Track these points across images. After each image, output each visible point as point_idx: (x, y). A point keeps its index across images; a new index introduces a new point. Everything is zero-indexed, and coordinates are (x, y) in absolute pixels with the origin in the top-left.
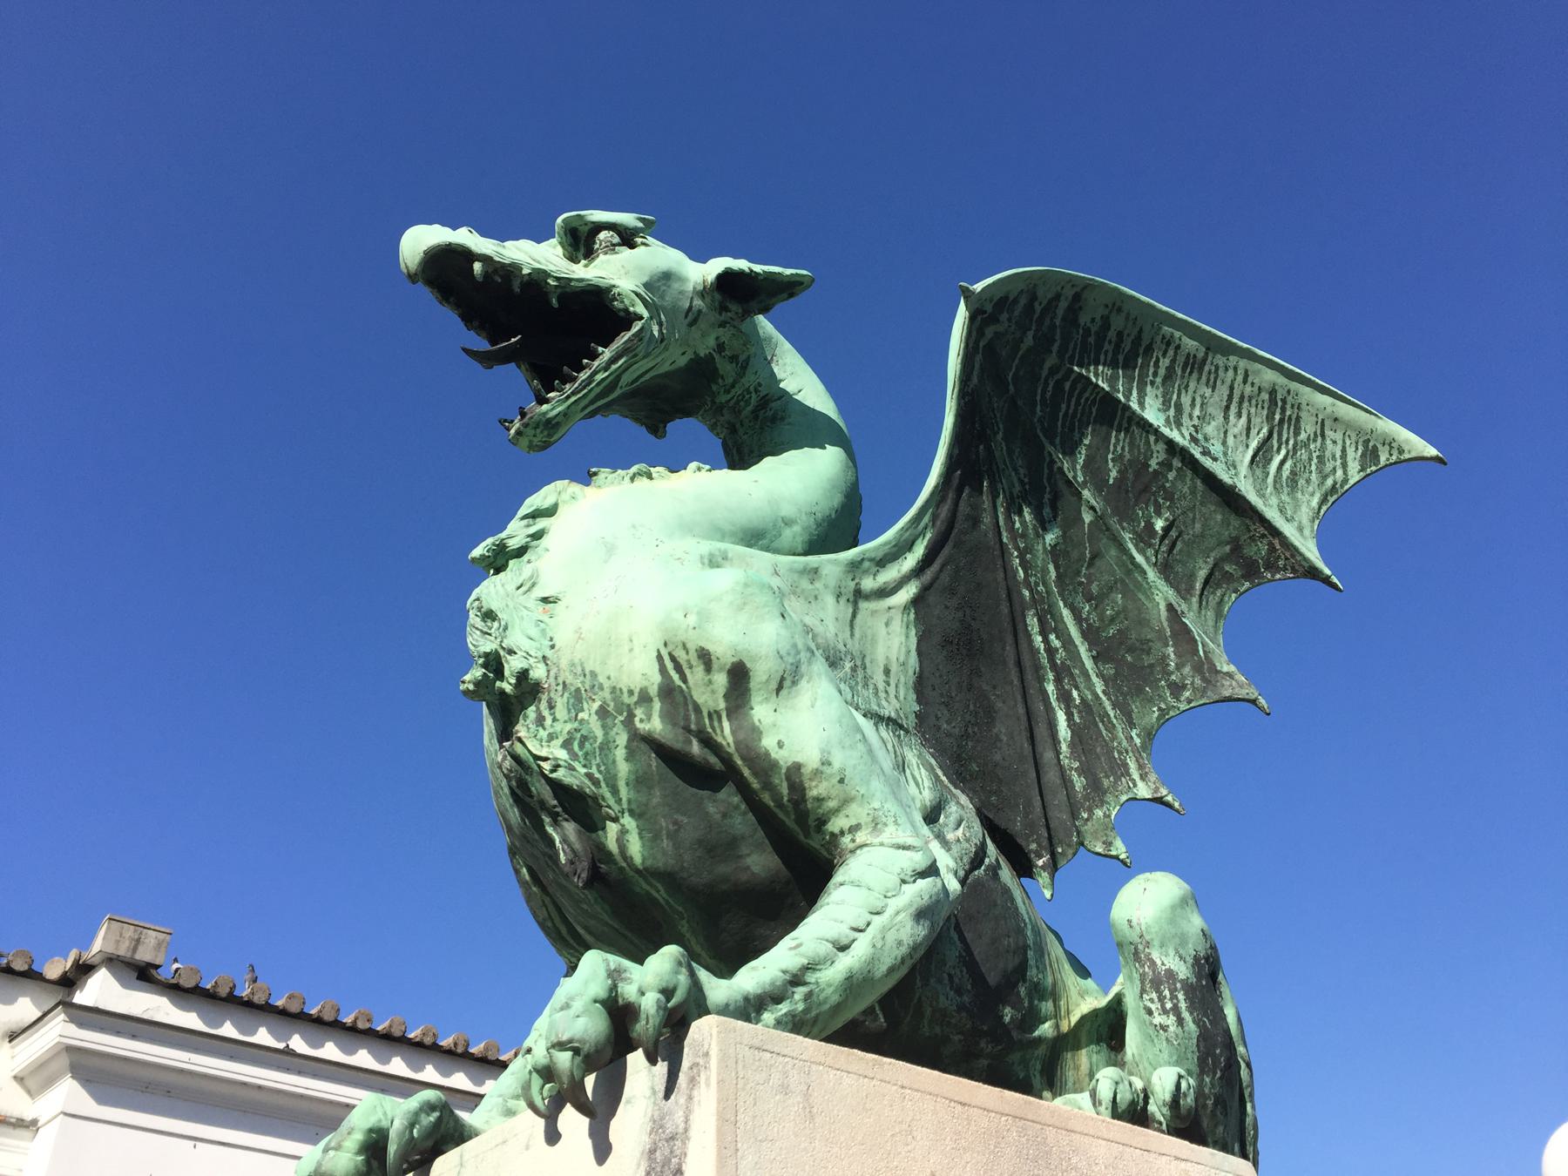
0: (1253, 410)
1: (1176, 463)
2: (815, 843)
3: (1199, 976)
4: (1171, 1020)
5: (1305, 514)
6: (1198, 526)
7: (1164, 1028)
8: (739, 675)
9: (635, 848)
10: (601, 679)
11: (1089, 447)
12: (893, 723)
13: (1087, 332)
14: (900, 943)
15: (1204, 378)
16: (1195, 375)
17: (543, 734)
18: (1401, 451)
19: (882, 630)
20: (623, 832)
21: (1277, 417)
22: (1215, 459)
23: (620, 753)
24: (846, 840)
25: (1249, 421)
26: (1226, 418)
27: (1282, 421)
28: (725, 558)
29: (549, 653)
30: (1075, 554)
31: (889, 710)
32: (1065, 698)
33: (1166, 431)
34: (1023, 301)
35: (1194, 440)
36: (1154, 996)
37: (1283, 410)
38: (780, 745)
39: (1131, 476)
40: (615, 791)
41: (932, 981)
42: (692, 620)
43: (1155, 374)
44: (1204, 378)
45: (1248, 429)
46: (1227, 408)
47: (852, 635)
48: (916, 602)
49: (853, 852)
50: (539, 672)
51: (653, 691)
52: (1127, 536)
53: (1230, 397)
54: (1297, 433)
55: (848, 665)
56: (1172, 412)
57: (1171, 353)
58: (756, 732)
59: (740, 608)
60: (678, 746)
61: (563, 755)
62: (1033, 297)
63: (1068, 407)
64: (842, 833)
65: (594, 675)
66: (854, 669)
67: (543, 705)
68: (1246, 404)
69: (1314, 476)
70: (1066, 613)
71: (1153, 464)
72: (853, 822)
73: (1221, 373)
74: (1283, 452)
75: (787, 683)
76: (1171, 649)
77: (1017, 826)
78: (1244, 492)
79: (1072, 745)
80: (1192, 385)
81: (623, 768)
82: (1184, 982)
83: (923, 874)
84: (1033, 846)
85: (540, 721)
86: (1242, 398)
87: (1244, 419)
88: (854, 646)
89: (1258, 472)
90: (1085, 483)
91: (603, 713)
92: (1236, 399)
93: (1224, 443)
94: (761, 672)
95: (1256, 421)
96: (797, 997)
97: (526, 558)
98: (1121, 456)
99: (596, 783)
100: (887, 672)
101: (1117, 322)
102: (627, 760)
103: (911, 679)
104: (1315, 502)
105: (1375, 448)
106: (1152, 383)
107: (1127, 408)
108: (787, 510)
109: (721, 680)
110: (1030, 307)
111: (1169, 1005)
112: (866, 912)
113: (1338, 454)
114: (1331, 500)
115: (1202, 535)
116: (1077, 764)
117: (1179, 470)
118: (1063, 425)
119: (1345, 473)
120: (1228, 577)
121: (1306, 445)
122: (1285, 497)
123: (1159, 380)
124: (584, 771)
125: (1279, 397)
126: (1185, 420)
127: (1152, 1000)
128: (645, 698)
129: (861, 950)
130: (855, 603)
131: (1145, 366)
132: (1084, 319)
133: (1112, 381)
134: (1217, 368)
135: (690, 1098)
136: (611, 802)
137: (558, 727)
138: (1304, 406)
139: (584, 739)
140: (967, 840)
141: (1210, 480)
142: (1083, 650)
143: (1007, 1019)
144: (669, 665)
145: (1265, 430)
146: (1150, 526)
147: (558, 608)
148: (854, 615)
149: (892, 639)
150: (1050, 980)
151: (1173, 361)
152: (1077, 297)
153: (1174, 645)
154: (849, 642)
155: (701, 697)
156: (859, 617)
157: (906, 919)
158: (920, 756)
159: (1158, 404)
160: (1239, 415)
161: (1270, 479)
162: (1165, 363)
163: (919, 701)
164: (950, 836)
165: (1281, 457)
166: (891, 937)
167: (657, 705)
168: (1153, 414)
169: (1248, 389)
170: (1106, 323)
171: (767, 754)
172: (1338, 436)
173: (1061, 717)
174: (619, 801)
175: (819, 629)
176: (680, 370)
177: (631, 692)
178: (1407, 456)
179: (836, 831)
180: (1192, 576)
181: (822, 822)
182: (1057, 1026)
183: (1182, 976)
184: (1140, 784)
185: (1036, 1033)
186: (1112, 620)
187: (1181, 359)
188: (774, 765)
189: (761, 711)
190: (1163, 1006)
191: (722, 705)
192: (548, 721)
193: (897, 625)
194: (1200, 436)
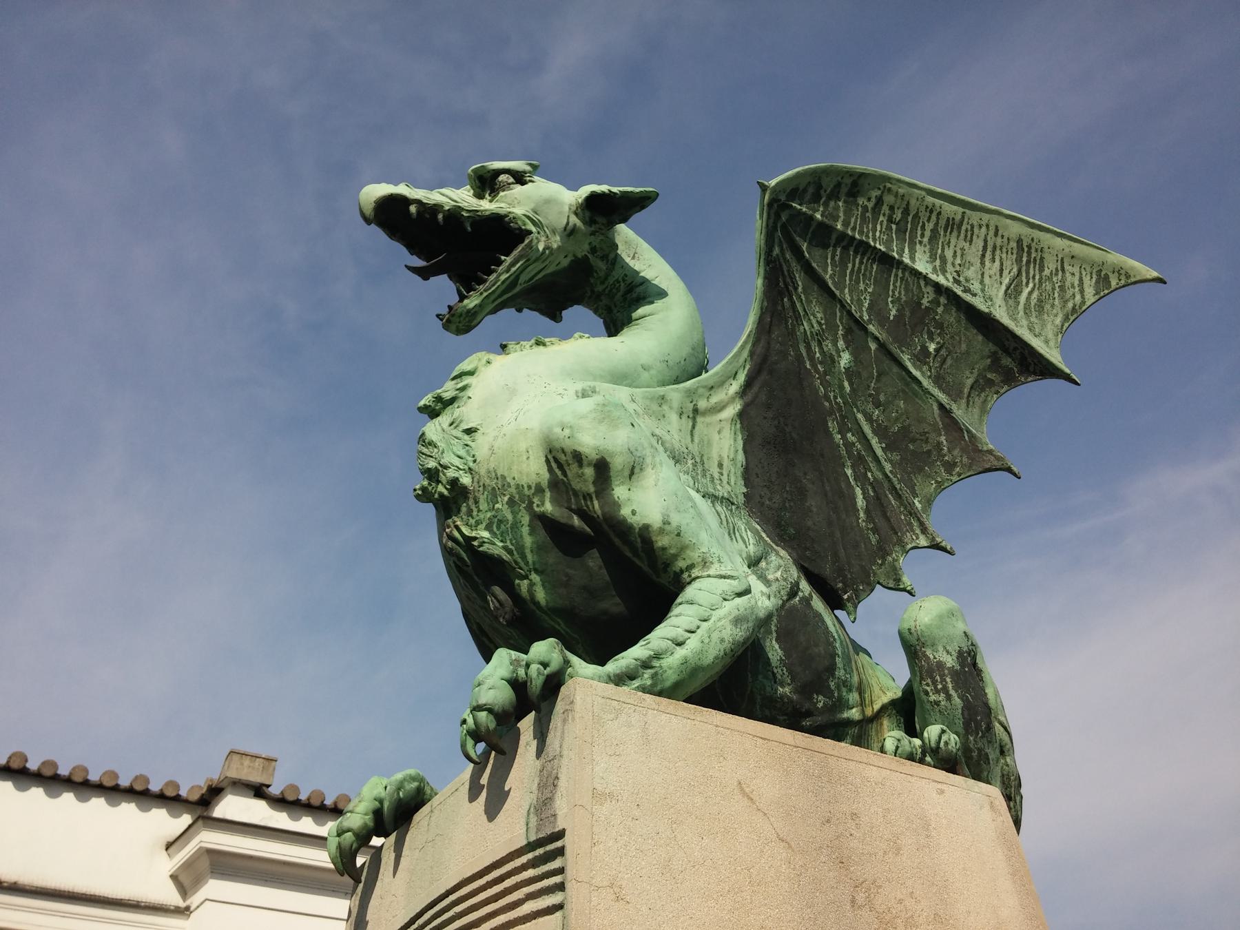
0: (1004, 256)
1: (943, 300)
2: (664, 580)
3: (962, 664)
4: (942, 697)
5: (1050, 331)
6: (964, 346)
7: (937, 703)
9: (541, 595)
10: (508, 480)
11: (871, 294)
13: (865, 208)
14: (722, 640)
15: (962, 235)
16: (955, 233)
17: (472, 521)
18: (1128, 276)
19: (716, 437)
20: (532, 584)
21: (1025, 259)
22: (975, 295)
23: (525, 530)
24: (685, 575)
25: (1002, 264)
26: (983, 263)
27: (1028, 262)
28: (594, 392)
29: (471, 464)
30: (865, 374)
31: (722, 491)
32: (861, 478)
33: (933, 277)
34: (811, 190)
36: (929, 681)
37: (1029, 253)
38: (634, 512)
40: (523, 557)
41: (760, 677)
42: (567, 432)
43: (923, 235)
44: (962, 235)
45: (1001, 270)
46: (983, 256)
47: (692, 440)
48: (741, 415)
49: (689, 583)
50: (466, 480)
51: (545, 484)
52: (906, 359)
53: (985, 248)
54: (1041, 270)
55: (690, 462)
56: (938, 263)
57: (934, 217)
58: (617, 505)
59: (601, 422)
60: (563, 521)
61: (486, 534)
62: (819, 187)
63: (854, 265)
64: (682, 571)
65: (504, 477)
66: (695, 465)
67: (471, 502)
68: (998, 252)
69: (1057, 302)
70: (859, 416)
71: (925, 302)
72: (689, 562)
73: (976, 230)
74: (1031, 285)
75: (637, 470)
76: (943, 439)
77: (827, 570)
78: (998, 317)
79: (867, 511)
80: (953, 242)
81: (528, 541)
82: (951, 669)
83: (740, 595)
84: (840, 585)
86: (995, 248)
87: (997, 263)
88: (694, 449)
89: (1011, 302)
90: (870, 321)
91: (511, 503)
92: (989, 249)
93: (982, 282)
94: (618, 463)
95: (1007, 264)
96: (646, 676)
97: (456, 405)
98: (899, 299)
99: (510, 552)
100: (720, 465)
101: (889, 199)
102: (530, 534)
103: (740, 471)
104: (1058, 321)
105: (1107, 277)
106: (921, 242)
108: (645, 359)
109: (589, 472)
111: (940, 687)
112: (700, 624)
113: (1076, 283)
114: (1072, 318)
115: (967, 353)
116: (871, 526)
117: (945, 305)
118: (851, 280)
119: (1083, 297)
120: (990, 383)
121: (1049, 278)
122: (1033, 319)
123: (926, 240)
124: (501, 544)
125: (1025, 244)
126: (949, 267)
127: (928, 685)
128: (539, 490)
129: (693, 643)
130: (694, 419)
131: (914, 230)
133: (888, 243)
134: (972, 226)
135: (563, 732)
136: (522, 564)
137: (482, 516)
138: (1046, 249)
139: (500, 522)
140: (785, 580)
142: (874, 441)
143: (820, 705)
144: (554, 465)
145: (1015, 270)
146: (925, 349)
147: (477, 435)
148: (693, 427)
149: (724, 443)
150: (856, 679)
151: (937, 224)
152: (855, 184)
153: (946, 434)
154: (690, 446)
155: (576, 485)
156: (697, 428)
157: (726, 623)
159: (926, 257)
162: (929, 227)
163: (746, 485)
164: (770, 577)
165: (1029, 289)
166: (715, 636)
167: (548, 494)
168: (922, 265)
169: (999, 240)
170: (880, 201)
171: (625, 520)
172: (1076, 270)
173: (858, 491)
174: (527, 563)
175: (667, 437)
176: (565, 270)
177: (529, 487)
178: (1133, 280)
179: (678, 570)
180: (962, 385)
181: (667, 565)
182: (863, 711)
183: (949, 665)
184: (922, 537)
185: (845, 715)
186: (897, 419)
187: (942, 223)
188: (630, 527)
189: (620, 492)
190: (936, 687)
191: (592, 489)
192: (475, 513)
193: (727, 433)
194: (961, 279)
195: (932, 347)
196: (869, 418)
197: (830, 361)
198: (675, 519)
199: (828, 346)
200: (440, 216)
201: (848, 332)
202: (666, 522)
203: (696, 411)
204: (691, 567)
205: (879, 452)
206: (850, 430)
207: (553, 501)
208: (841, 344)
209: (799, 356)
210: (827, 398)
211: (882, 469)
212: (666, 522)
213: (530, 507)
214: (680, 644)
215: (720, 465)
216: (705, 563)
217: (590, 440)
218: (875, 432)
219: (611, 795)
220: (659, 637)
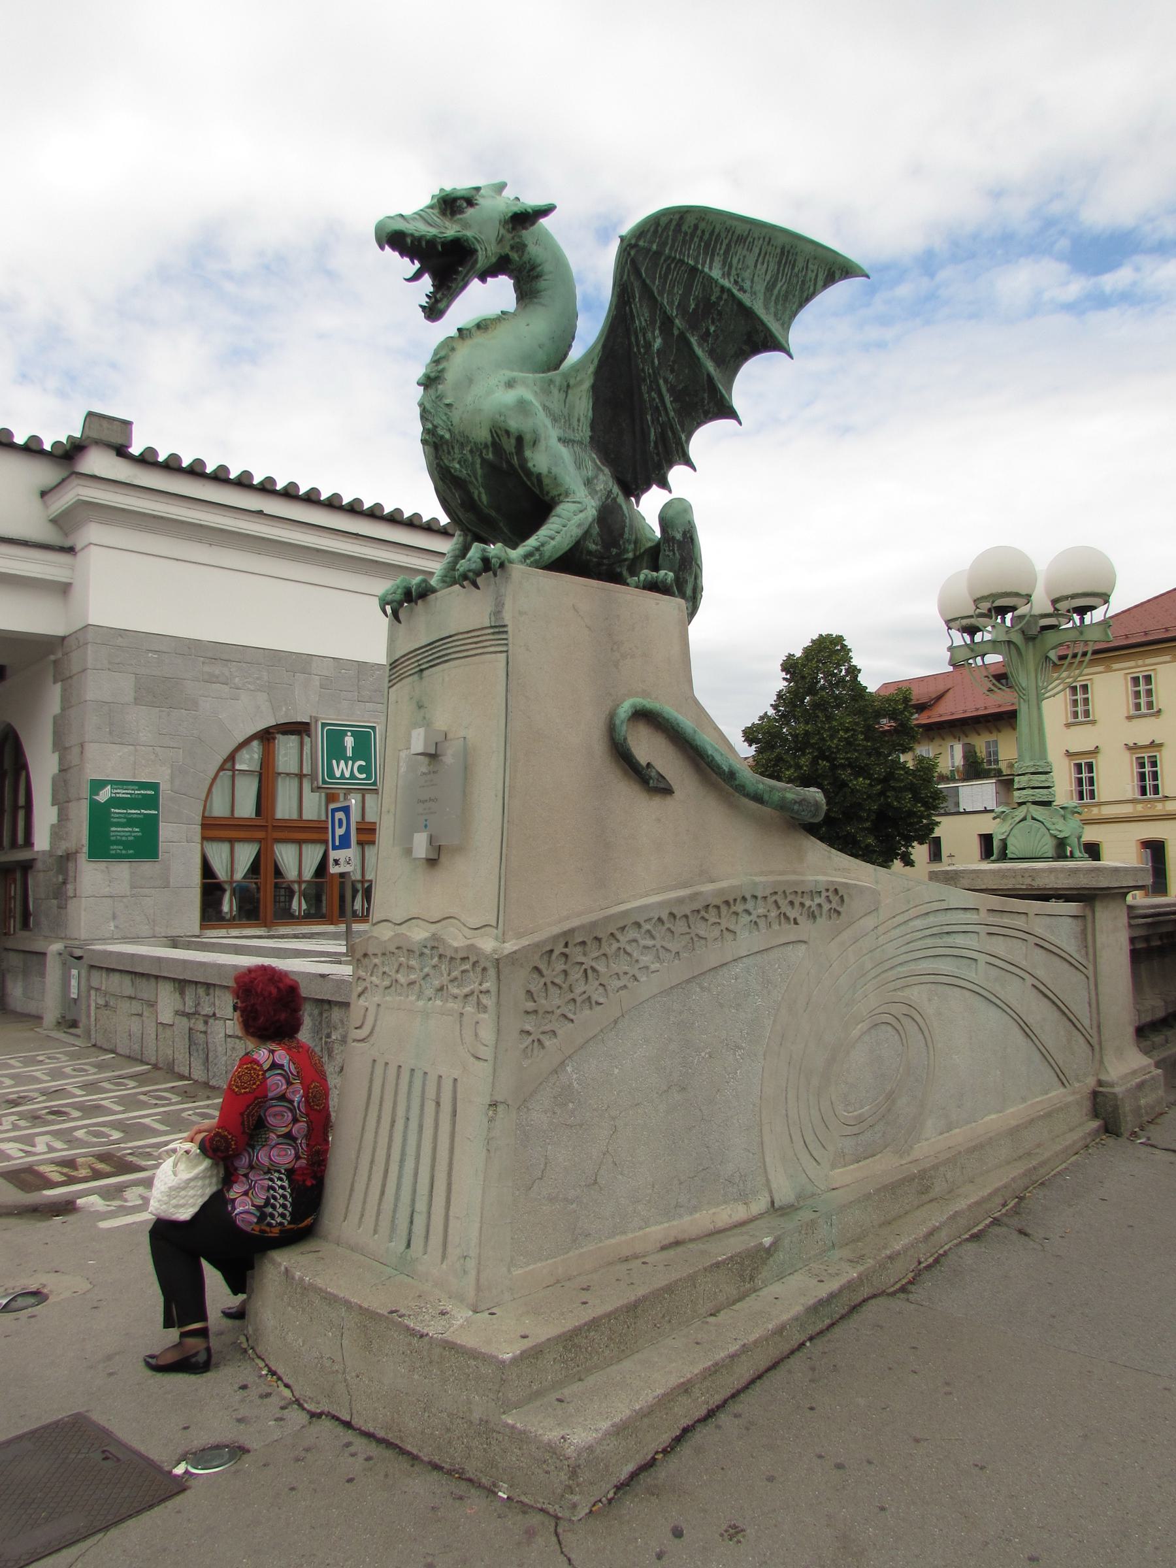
1: (725, 296)
2: (547, 498)
8: (520, 440)
12: (580, 443)
20: (480, 493)
22: (745, 292)
23: (478, 466)
26: (756, 266)
33: (721, 281)
35: (736, 282)
39: (701, 306)
48: (594, 387)
50: (447, 436)
51: (489, 443)
52: (693, 340)
53: (759, 254)
54: (793, 268)
61: (457, 466)
70: (661, 382)
71: (713, 298)
79: (656, 443)
81: (479, 472)
85: (449, 453)
91: (471, 451)
94: (528, 438)
100: (579, 420)
101: (702, 225)
103: (589, 421)
107: (702, 271)
109: (513, 441)
110: (656, 231)
112: (562, 528)
122: (779, 307)
126: (733, 272)
128: (486, 446)
129: (558, 538)
132: (685, 228)
141: (740, 304)
142: (668, 399)
146: (708, 330)
152: (681, 218)
155: (506, 447)
157: (574, 528)
158: (590, 456)
160: (763, 263)
161: (773, 298)
162: (726, 242)
168: (716, 273)
170: (696, 227)
173: (652, 430)
175: (551, 406)
181: (548, 493)
187: (735, 238)
189: (528, 453)
195: (712, 329)
196: (666, 381)
197: (648, 345)
198: (554, 470)
199: (649, 335)
200: (424, 243)
201: (662, 324)
202: (550, 472)
203: (568, 386)
204: (560, 495)
205: (669, 405)
206: (653, 390)
207: (494, 453)
208: (657, 332)
209: (630, 344)
210: (643, 370)
211: (667, 414)
212: (550, 472)
213: (481, 455)
214: (553, 539)
215: (579, 420)
216: (567, 494)
217: (514, 424)
218: (668, 390)
219: (525, 613)
220: (543, 532)
